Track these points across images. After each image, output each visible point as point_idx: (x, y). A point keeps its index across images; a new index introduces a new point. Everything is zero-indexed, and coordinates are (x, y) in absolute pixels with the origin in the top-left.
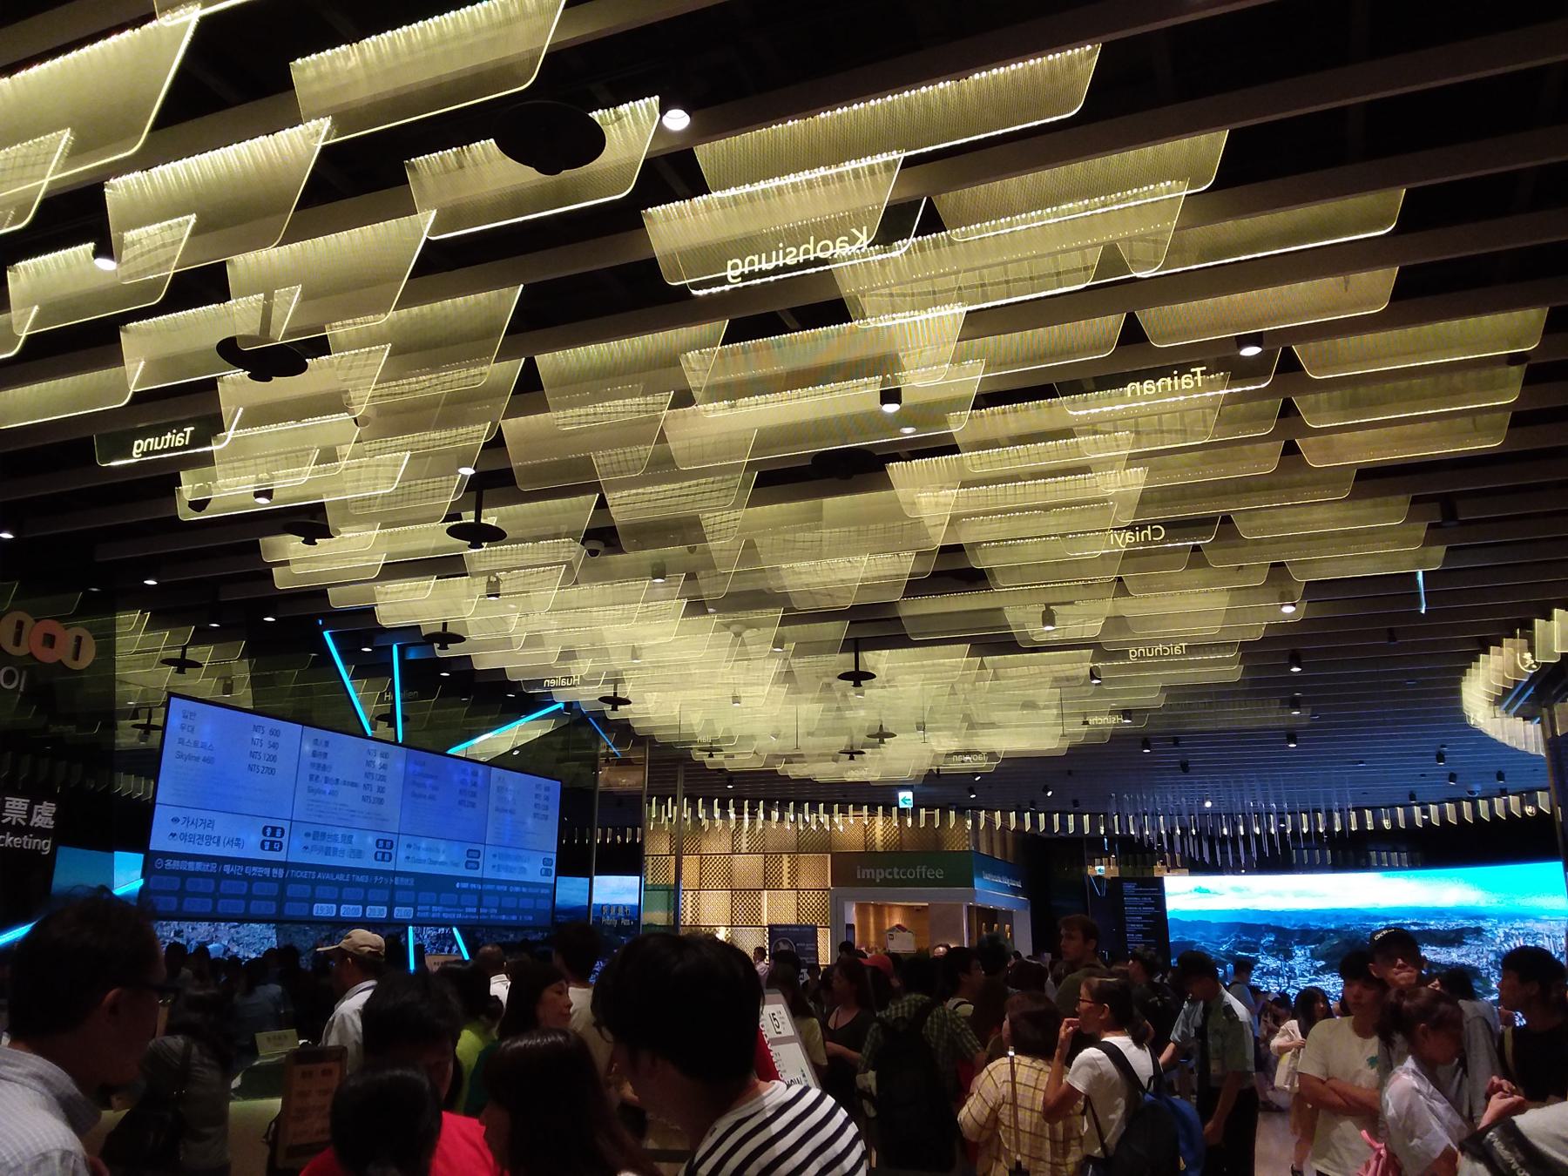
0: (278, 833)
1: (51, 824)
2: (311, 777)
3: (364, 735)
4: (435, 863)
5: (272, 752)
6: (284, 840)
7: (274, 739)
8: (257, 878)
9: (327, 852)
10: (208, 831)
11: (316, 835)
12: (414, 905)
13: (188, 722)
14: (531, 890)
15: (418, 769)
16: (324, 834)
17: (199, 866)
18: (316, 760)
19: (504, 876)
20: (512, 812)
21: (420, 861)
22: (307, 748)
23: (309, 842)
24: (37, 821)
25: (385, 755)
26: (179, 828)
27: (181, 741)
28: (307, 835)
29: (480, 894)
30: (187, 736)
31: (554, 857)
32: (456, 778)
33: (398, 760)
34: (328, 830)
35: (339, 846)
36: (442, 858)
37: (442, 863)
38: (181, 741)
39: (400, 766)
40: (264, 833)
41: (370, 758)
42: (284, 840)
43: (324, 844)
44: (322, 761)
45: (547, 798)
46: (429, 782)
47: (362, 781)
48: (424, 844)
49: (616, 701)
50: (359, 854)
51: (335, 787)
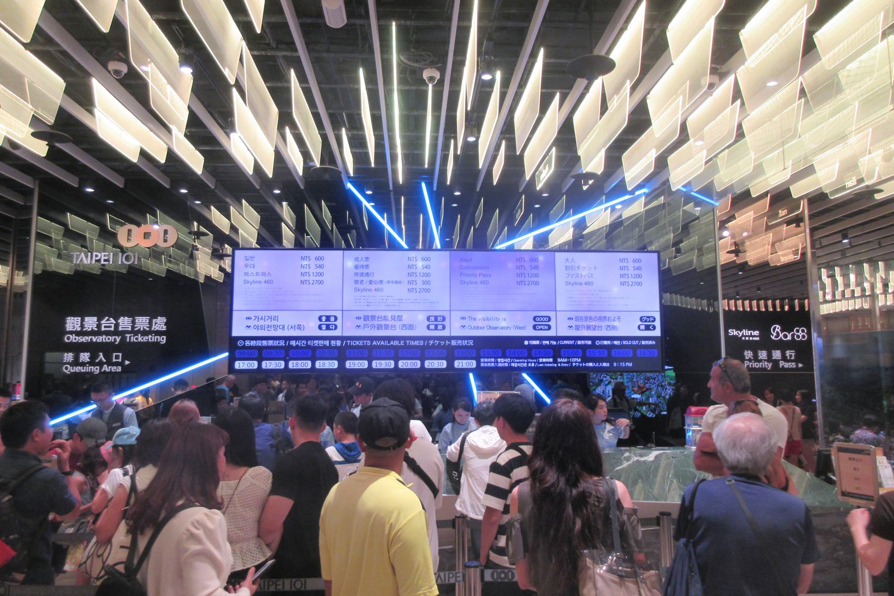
0: (332, 319)
1: (164, 328)
2: (356, 282)
4: (496, 328)
7: (319, 263)
8: (319, 347)
9: (379, 327)
10: (274, 323)
11: (366, 318)
13: (249, 262)
14: (625, 343)
16: (373, 317)
17: (271, 343)
18: (360, 271)
22: (350, 264)
23: (361, 322)
24: (155, 328)
26: (251, 323)
27: (246, 274)
30: (250, 270)
34: (377, 314)
35: (390, 323)
36: (504, 324)
37: (502, 328)
38: (246, 274)
40: (320, 319)
41: (411, 263)
43: (376, 323)
44: (365, 271)
46: (479, 272)
48: (480, 315)
50: (411, 327)
51: (379, 286)
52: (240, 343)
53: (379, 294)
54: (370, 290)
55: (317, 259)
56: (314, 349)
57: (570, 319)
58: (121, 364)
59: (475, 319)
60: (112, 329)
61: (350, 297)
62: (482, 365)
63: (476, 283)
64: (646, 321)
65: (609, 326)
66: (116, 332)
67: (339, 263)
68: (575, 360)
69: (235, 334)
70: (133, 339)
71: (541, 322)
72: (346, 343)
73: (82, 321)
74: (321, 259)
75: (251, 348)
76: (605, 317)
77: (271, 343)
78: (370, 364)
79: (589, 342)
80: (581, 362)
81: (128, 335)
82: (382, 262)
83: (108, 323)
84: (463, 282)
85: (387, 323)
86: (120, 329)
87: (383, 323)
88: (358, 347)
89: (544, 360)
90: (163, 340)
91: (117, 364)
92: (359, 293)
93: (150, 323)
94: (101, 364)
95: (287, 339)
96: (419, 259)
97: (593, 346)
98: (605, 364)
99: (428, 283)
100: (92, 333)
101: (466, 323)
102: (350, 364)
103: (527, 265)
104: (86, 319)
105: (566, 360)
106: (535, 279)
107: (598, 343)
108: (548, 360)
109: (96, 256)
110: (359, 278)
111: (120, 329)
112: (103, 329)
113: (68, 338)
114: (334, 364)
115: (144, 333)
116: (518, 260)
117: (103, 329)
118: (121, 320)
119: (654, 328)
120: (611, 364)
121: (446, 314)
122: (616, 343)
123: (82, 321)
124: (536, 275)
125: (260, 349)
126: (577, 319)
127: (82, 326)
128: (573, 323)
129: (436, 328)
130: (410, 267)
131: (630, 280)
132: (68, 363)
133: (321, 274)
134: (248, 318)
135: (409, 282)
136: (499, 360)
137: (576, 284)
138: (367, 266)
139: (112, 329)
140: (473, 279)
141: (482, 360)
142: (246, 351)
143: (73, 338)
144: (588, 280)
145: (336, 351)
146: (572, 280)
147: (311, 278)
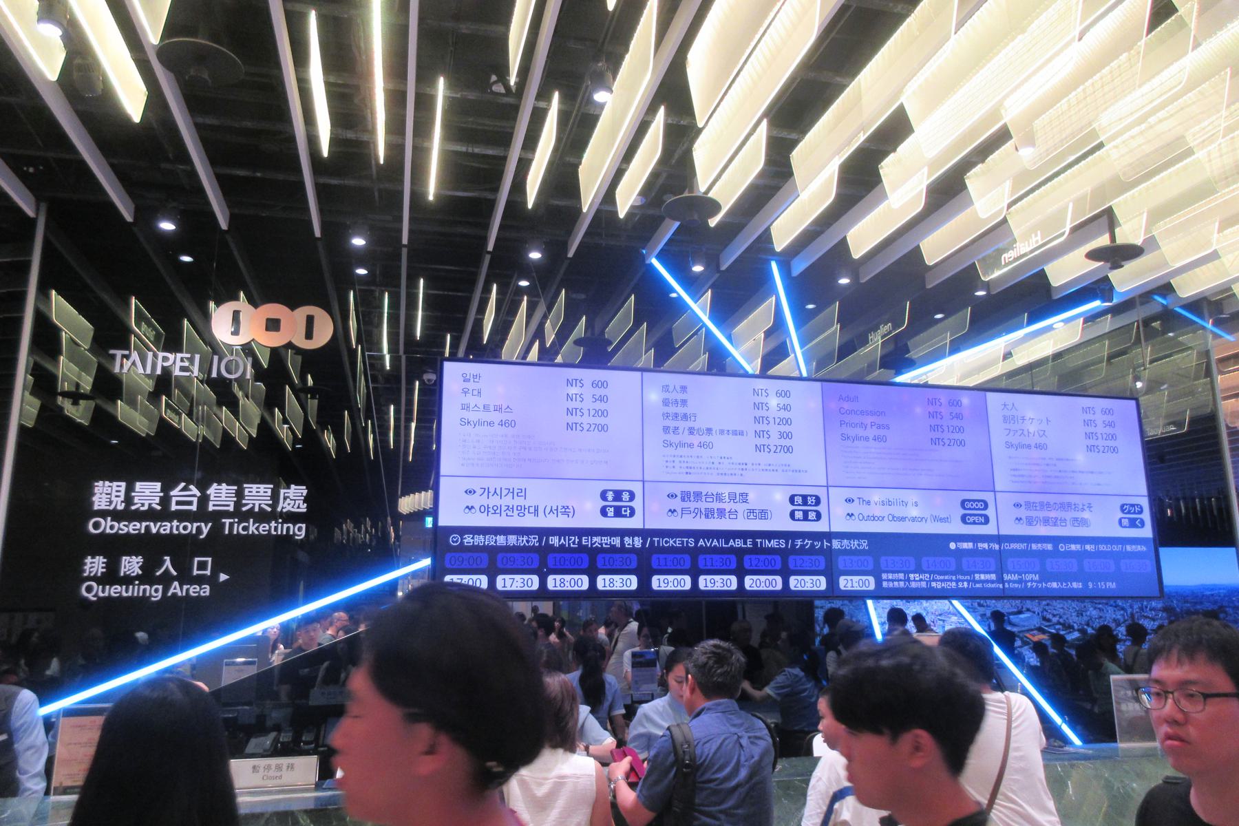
0: (626, 496)
1: (303, 508)
2: (666, 429)
4: (903, 519)
7: (600, 392)
8: (601, 550)
9: (709, 514)
10: (519, 501)
11: (685, 496)
13: (471, 386)
14: (1102, 547)
16: (698, 495)
17: (512, 540)
18: (672, 409)
22: (654, 397)
23: (677, 504)
24: (285, 506)
27: (465, 407)
29: (1000, 556)
30: (471, 400)
31: (1145, 503)
34: (704, 489)
36: (914, 512)
37: (914, 519)
38: (465, 407)
40: (603, 496)
41: (758, 399)
42: (637, 504)
43: (703, 505)
44: (680, 410)
45: (1111, 424)
46: (868, 420)
47: (751, 427)
48: (876, 496)
49: (1119, 255)
50: (763, 514)
51: (706, 438)
53: (702, 452)
54: (691, 445)
55: (595, 384)
56: (594, 552)
57: (1017, 505)
58: (212, 580)
59: (868, 503)
60: (194, 508)
61: (657, 460)
63: (867, 439)
64: (1129, 512)
65: (1076, 519)
66: (202, 514)
68: (1029, 577)
70: (238, 529)
71: (973, 510)
72: (652, 542)
73: (130, 489)
74: (603, 384)
75: (475, 549)
76: (1069, 504)
77: (512, 540)
78: (695, 583)
79: (1049, 547)
80: (1040, 581)
81: (227, 521)
82: (715, 399)
83: (184, 495)
84: (845, 437)
85: (721, 506)
86: (211, 508)
87: (716, 505)
88: (672, 550)
89: (983, 577)
90: (299, 531)
91: (200, 580)
92: (671, 451)
93: (275, 497)
94: (166, 580)
96: (772, 393)
97: (1055, 553)
98: (1075, 585)
99: (788, 436)
100: (151, 515)
101: (855, 508)
102: (660, 583)
103: (944, 410)
104: (138, 485)
105: (1016, 577)
107: (1062, 547)
108: (988, 577)
109: (165, 359)
110: (671, 423)
111: (211, 508)
112: (174, 507)
114: (630, 583)
115: (262, 517)
116: (931, 402)
117: (174, 507)
118: (212, 490)
119: (1143, 523)
120: (1085, 585)
121: (822, 493)
122: (1088, 547)
123: (130, 489)
124: (961, 430)
125: (493, 551)
126: (1029, 505)
127: (128, 500)
128: (1023, 513)
129: (806, 518)
130: (757, 406)
131: (1100, 443)
133: (604, 413)
134: (470, 492)
135: (757, 434)
136: (912, 576)
137: (1023, 446)
138: (684, 402)
139: (194, 508)
140: (860, 432)
141: (884, 576)
142: (466, 556)
143: (108, 526)
146: (1015, 440)
147: (586, 420)
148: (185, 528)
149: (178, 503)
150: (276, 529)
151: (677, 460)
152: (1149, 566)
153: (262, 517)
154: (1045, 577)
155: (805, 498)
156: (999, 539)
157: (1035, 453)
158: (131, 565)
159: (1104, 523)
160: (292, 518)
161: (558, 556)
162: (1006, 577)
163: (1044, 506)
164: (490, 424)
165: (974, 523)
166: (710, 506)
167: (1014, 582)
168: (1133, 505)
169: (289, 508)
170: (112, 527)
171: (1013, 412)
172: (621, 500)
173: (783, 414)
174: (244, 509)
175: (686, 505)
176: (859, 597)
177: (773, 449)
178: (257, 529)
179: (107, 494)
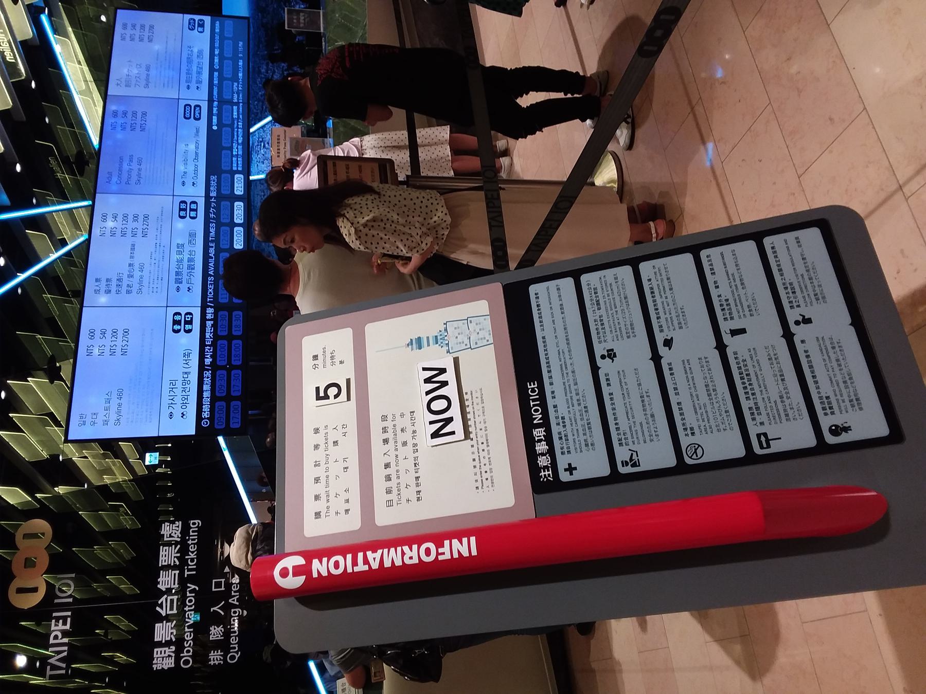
0: (177, 318)
2: (128, 292)
3: (88, 242)
4: (197, 154)
5: (109, 334)
6: (183, 311)
7: (98, 334)
8: (215, 333)
9: (191, 268)
11: (179, 281)
12: (233, 173)
13: (89, 420)
14: (217, 45)
15: (115, 179)
16: (177, 273)
17: (207, 387)
18: (114, 288)
19: (205, 76)
20: (148, 68)
21: (196, 171)
22: (103, 299)
25: (104, 218)
26: (177, 412)
27: (106, 423)
28: (178, 289)
29: (222, 102)
30: (100, 419)
31: (188, 17)
32: (120, 136)
33: (106, 203)
35: (186, 257)
36: (192, 147)
37: (197, 148)
38: (106, 423)
39: (113, 199)
40: (178, 331)
41: (108, 233)
42: (183, 311)
43: (185, 271)
44: (114, 283)
46: (125, 167)
47: (129, 240)
48: (181, 168)
50: (192, 235)
51: (136, 267)
52: (205, 424)
54: (141, 277)
57: (188, 87)
62: (240, 169)
63: (140, 170)
65: (198, 56)
67: (98, 313)
68: (235, 88)
69: (192, 432)
71: (191, 112)
77: (207, 387)
79: (216, 74)
81: (186, 573)
85: (186, 259)
93: (169, 544)
94: (228, 607)
95: (202, 367)
97: (220, 71)
105: (236, 95)
106: (139, 115)
107: (216, 67)
110: (124, 288)
113: (186, 662)
115: (184, 550)
118: (162, 587)
120: (241, 58)
122: (217, 52)
123: (160, 644)
124: (134, 114)
126: (188, 81)
127: (168, 644)
128: (193, 85)
129: (196, 210)
132: (225, 656)
133: (115, 332)
134: (171, 415)
136: (234, 153)
138: (108, 280)
141: (234, 168)
142: (217, 415)
144: (144, 68)
145: (220, 313)
148: (190, 601)
149: (171, 609)
150: (193, 540)
151: (151, 285)
152: (229, 23)
153: (184, 550)
154: (235, 79)
155: (181, 210)
156: (210, 101)
157: (153, 72)
158: (216, 632)
159: (201, 41)
160: (185, 531)
161: (218, 359)
162: (235, 100)
163: (189, 73)
164: (120, 405)
165: (200, 114)
166: (185, 266)
167: (238, 96)
168: (190, 23)
169: (178, 533)
170: (188, 651)
171: (123, 80)
172: (180, 321)
173: (120, 218)
174: (178, 563)
175: (184, 281)
176: (248, 184)
177: (145, 226)
178: (193, 552)
179: (163, 660)
